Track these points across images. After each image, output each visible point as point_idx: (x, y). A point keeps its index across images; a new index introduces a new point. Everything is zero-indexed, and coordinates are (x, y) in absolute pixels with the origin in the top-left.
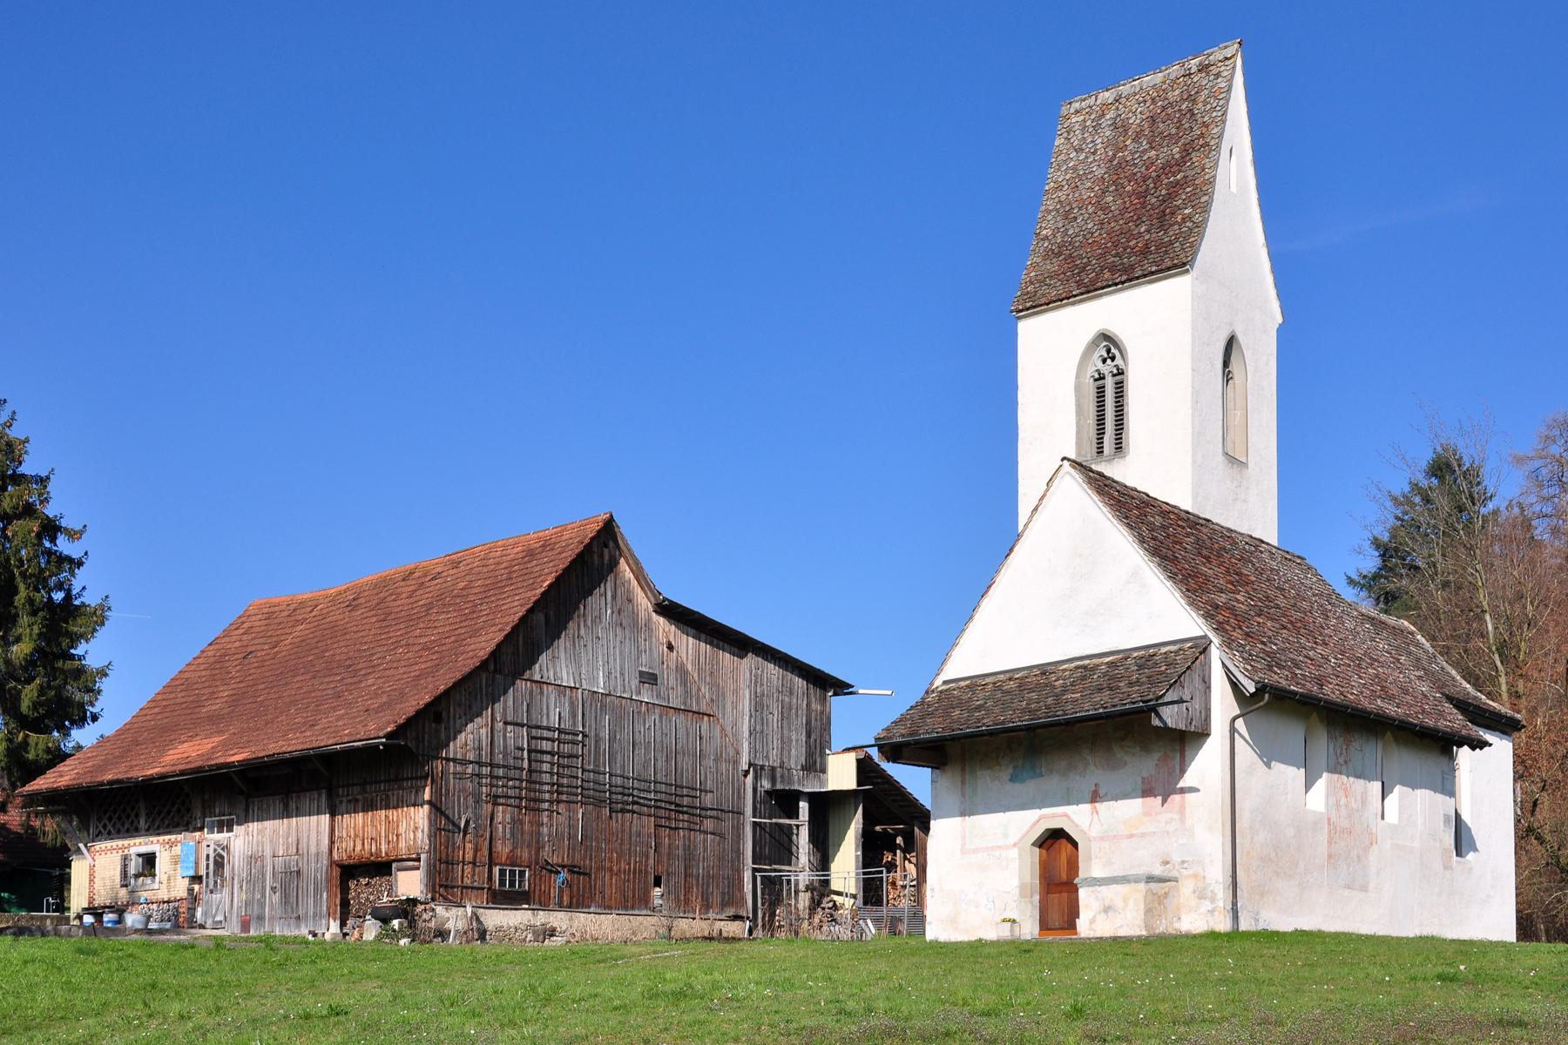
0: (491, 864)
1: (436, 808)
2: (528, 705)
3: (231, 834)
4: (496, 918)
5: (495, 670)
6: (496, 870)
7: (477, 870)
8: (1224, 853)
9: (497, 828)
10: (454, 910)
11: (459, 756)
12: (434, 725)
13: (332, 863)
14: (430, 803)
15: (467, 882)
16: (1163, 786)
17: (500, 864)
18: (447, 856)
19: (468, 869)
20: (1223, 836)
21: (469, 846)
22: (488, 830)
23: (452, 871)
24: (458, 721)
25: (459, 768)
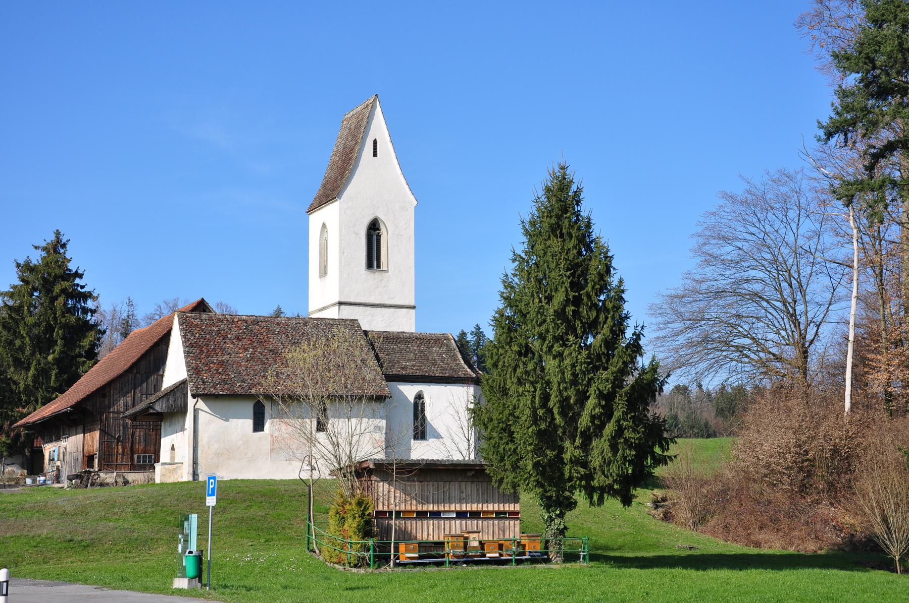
0: (133, 452)
1: (103, 433)
2: (155, 385)
3: (66, 443)
4: (132, 477)
5: (137, 373)
6: (136, 456)
7: (125, 457)
8: (189, 453)
9: (136, 438)
10: (110, 474)
11: (116, 410)
12: (102, 399)
13: (83, 456)
14: (100, 429)
15: (119, 462)
16: (183, 429)
17: (138, 453)
18: (109, 452)
19: (120, 457)
20: (189, 447)
21: (120, 447)
22: (131, 440)
23: (112, 458)
24: (115, 396)
25: (115, 415)
